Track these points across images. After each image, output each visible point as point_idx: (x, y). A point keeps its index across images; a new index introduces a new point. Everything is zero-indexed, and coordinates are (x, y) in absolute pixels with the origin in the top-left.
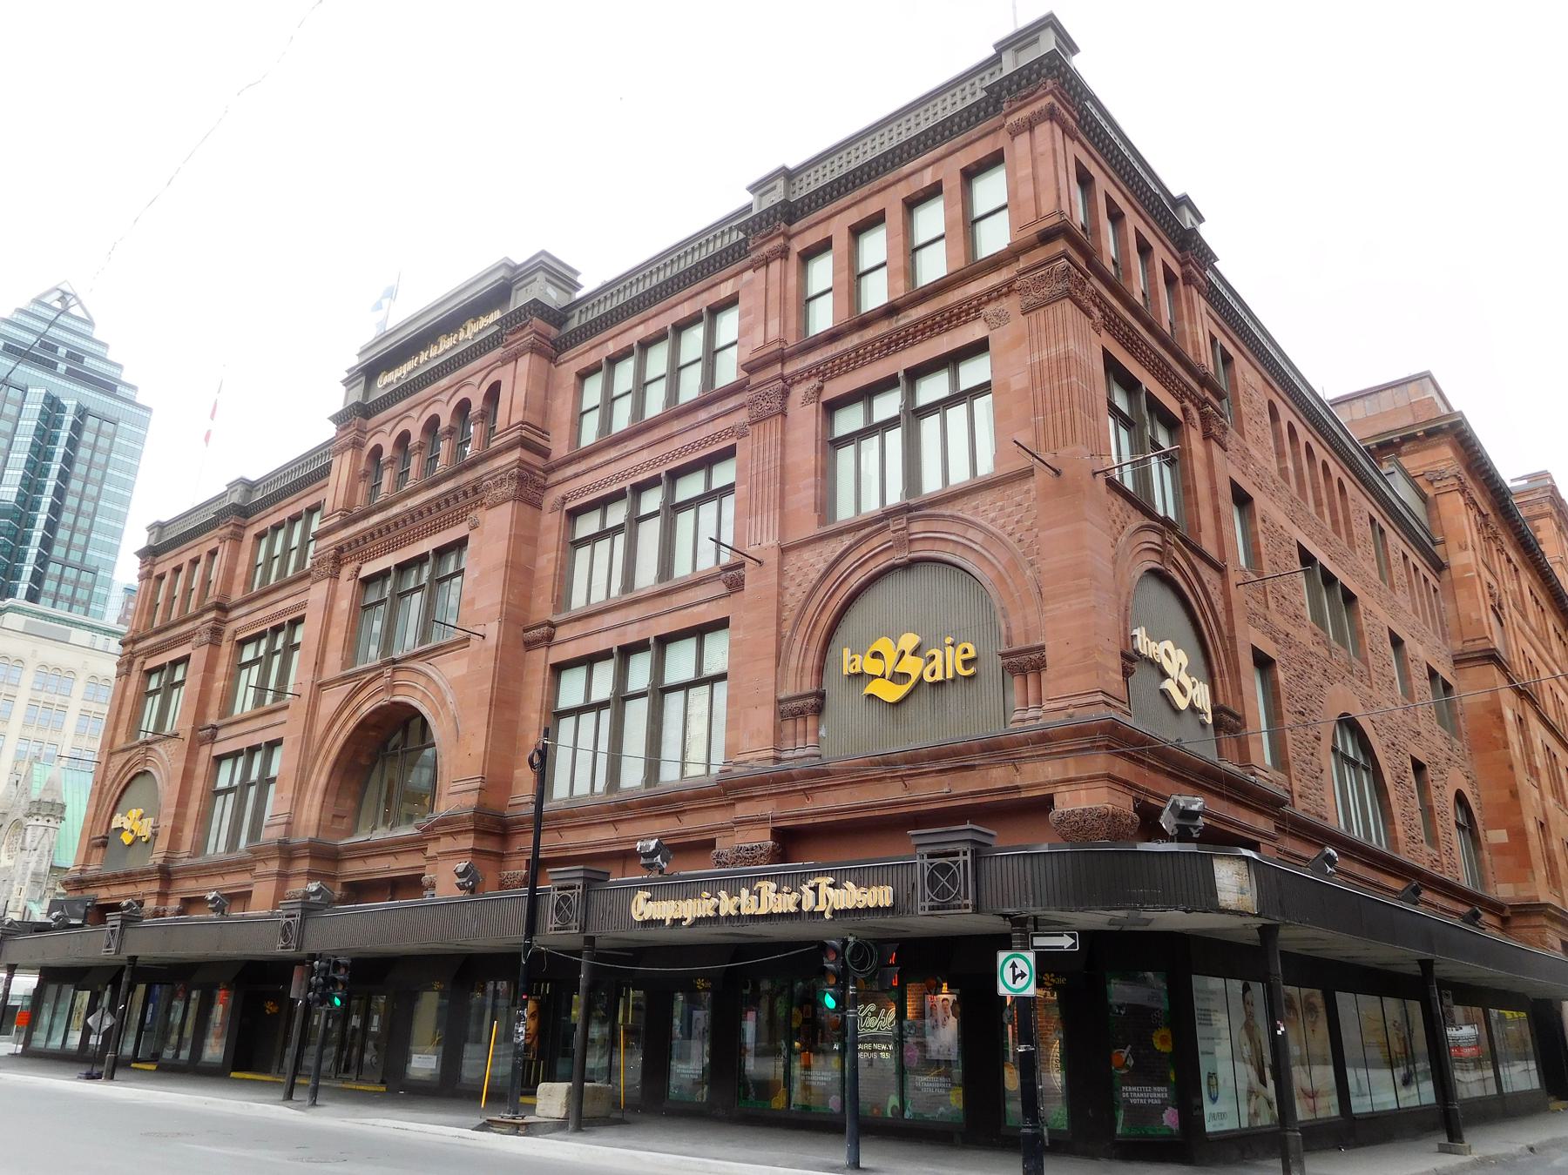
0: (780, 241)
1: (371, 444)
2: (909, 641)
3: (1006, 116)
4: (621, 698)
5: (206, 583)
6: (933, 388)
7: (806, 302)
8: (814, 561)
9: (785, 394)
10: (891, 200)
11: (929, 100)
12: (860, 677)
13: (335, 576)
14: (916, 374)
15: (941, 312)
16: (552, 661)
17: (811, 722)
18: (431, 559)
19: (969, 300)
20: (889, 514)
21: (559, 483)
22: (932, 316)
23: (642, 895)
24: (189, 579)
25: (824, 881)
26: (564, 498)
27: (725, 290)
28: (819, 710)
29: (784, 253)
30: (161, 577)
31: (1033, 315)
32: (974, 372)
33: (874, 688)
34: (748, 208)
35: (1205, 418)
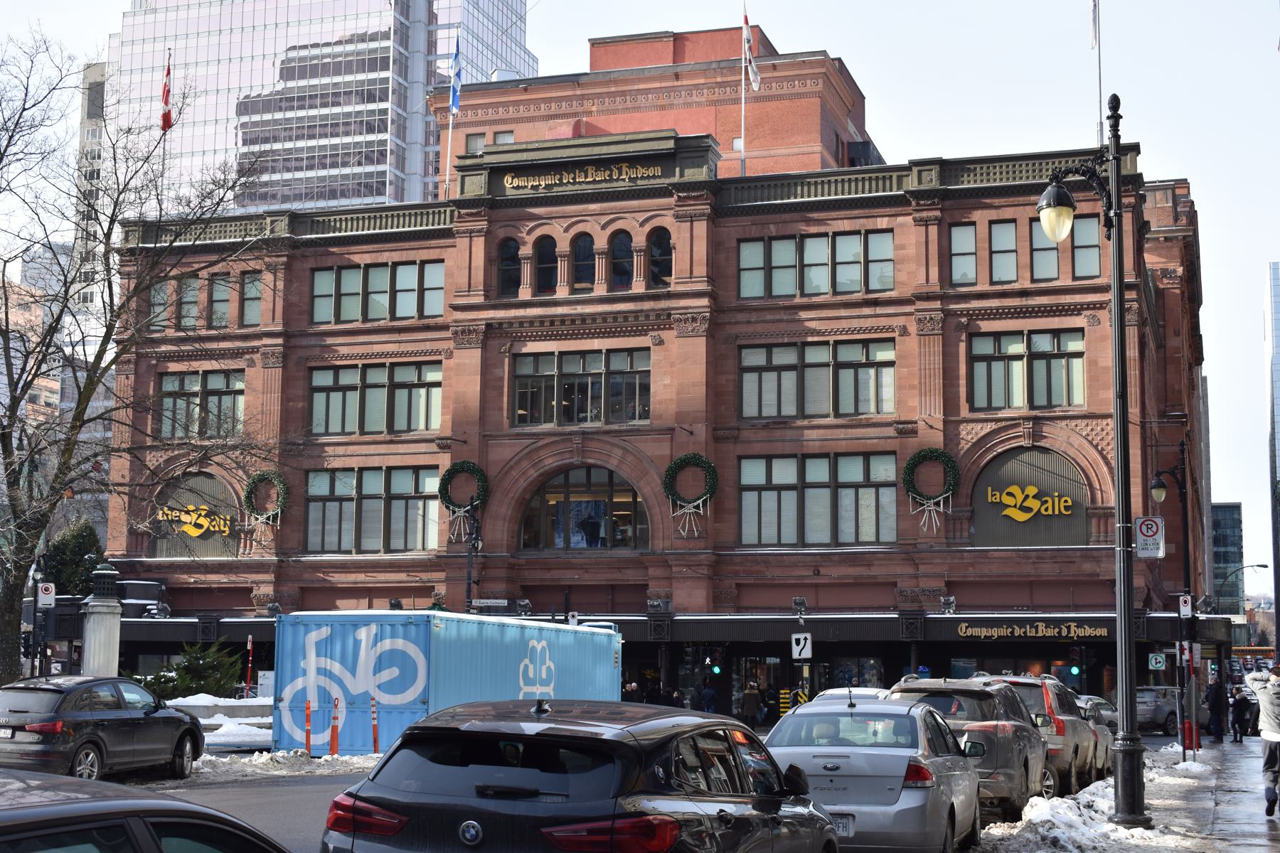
4: (802, 487)
15: (1057, 305)
16: (738, 453)
19: (1076, 305)
21: (730, 323)
23: (964, 625)
25: (1073, 625)
27: (883, 223)
33: (1006, 512)
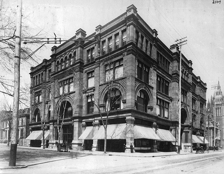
1: (57, 60)
5: (42, 78)
6: (117, 65)
9: (100, 64)
24: (36, 79)
30: (34, 77)
34: (95, 33)
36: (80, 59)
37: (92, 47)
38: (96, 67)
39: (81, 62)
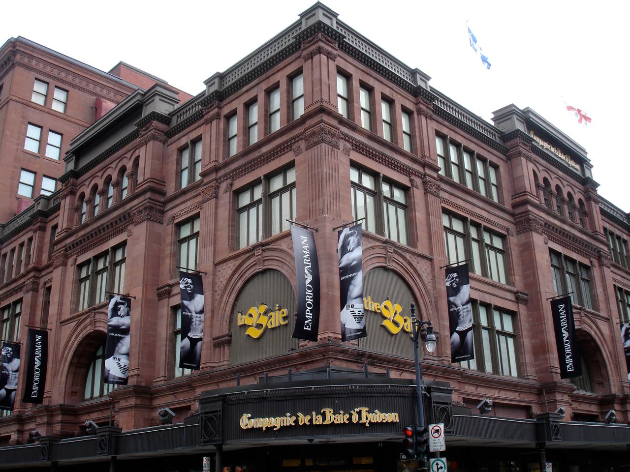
0: (216, 110)
2: (263, 308)
3: (303, 50)
6: (277, 184)
7: (228, 140)
8: (227, 270)
9: (218, 187)
10: (281, 77)
11: (266, 47)
12: (245, 326)
13: (65, 264)
14: (269, 177)
17: (226, 348)
18: (110, 253)
20: (255, 247)
22: (273, 150)
26: (174, 217)
28: (229, 342)
29: (218, 116)
31: (310, 150)
32: (292, 176)
35: (425, 183)
36: (152, 180)
37: (193, 135)
38: (204, 202)
39: (156, 188)
